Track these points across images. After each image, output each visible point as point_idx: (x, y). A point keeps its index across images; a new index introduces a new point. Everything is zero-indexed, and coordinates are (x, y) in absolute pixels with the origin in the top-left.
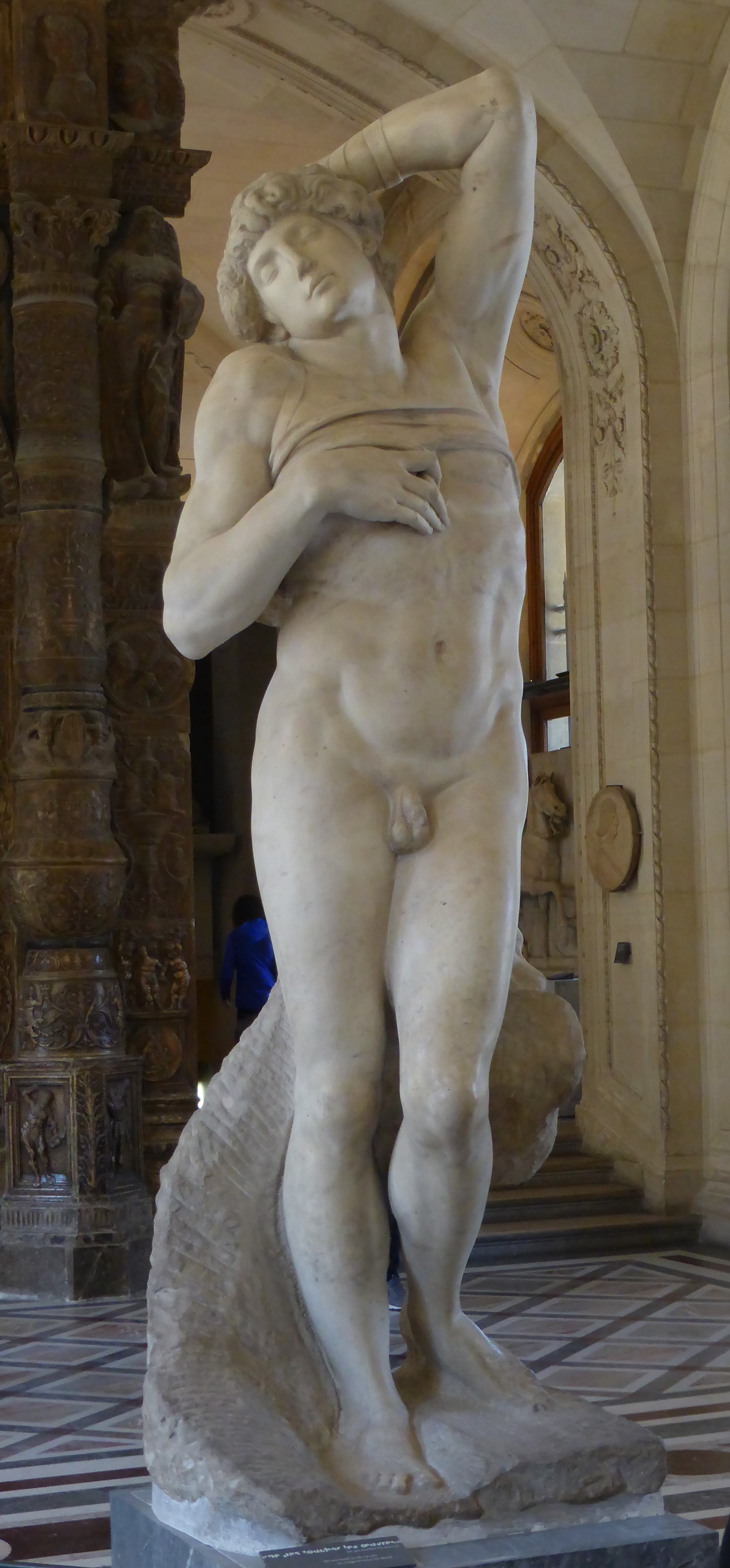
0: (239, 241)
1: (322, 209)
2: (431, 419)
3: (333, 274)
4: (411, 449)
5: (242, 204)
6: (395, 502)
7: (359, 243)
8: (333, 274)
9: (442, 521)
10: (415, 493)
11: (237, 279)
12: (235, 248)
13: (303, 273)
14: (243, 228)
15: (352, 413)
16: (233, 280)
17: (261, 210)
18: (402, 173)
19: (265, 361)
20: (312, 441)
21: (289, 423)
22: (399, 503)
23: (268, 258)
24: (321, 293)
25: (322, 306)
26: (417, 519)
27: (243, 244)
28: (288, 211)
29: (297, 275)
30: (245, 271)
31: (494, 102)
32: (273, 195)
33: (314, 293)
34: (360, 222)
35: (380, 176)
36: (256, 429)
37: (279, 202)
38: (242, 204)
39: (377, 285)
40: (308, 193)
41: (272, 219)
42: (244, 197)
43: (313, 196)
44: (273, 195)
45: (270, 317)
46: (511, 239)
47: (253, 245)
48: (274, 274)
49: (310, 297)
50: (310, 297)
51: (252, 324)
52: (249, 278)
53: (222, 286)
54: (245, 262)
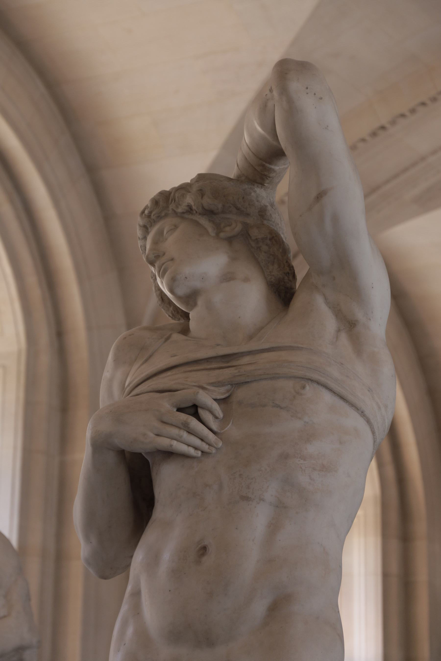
1: (180, 210)
2: (246, 360)
3: (172, 259)
4: (184, 389)
6: (151, 435)
7: (210, 230)
8: (172, 259)
9: (209, 445)
10: (172, 425)
12: (143, 253)
15: (165, 367)
18: (270, 163)
19: (125, 338)
22: (158, 435)
26: (171, 446)
28: (160, 218)
34: (209, 213)
35: (255, 169)
37: (150, 212)
39: (233, 259)
41: (148, 226)
43: (173, 202)
46: (320, 196)
51: (171, 309)
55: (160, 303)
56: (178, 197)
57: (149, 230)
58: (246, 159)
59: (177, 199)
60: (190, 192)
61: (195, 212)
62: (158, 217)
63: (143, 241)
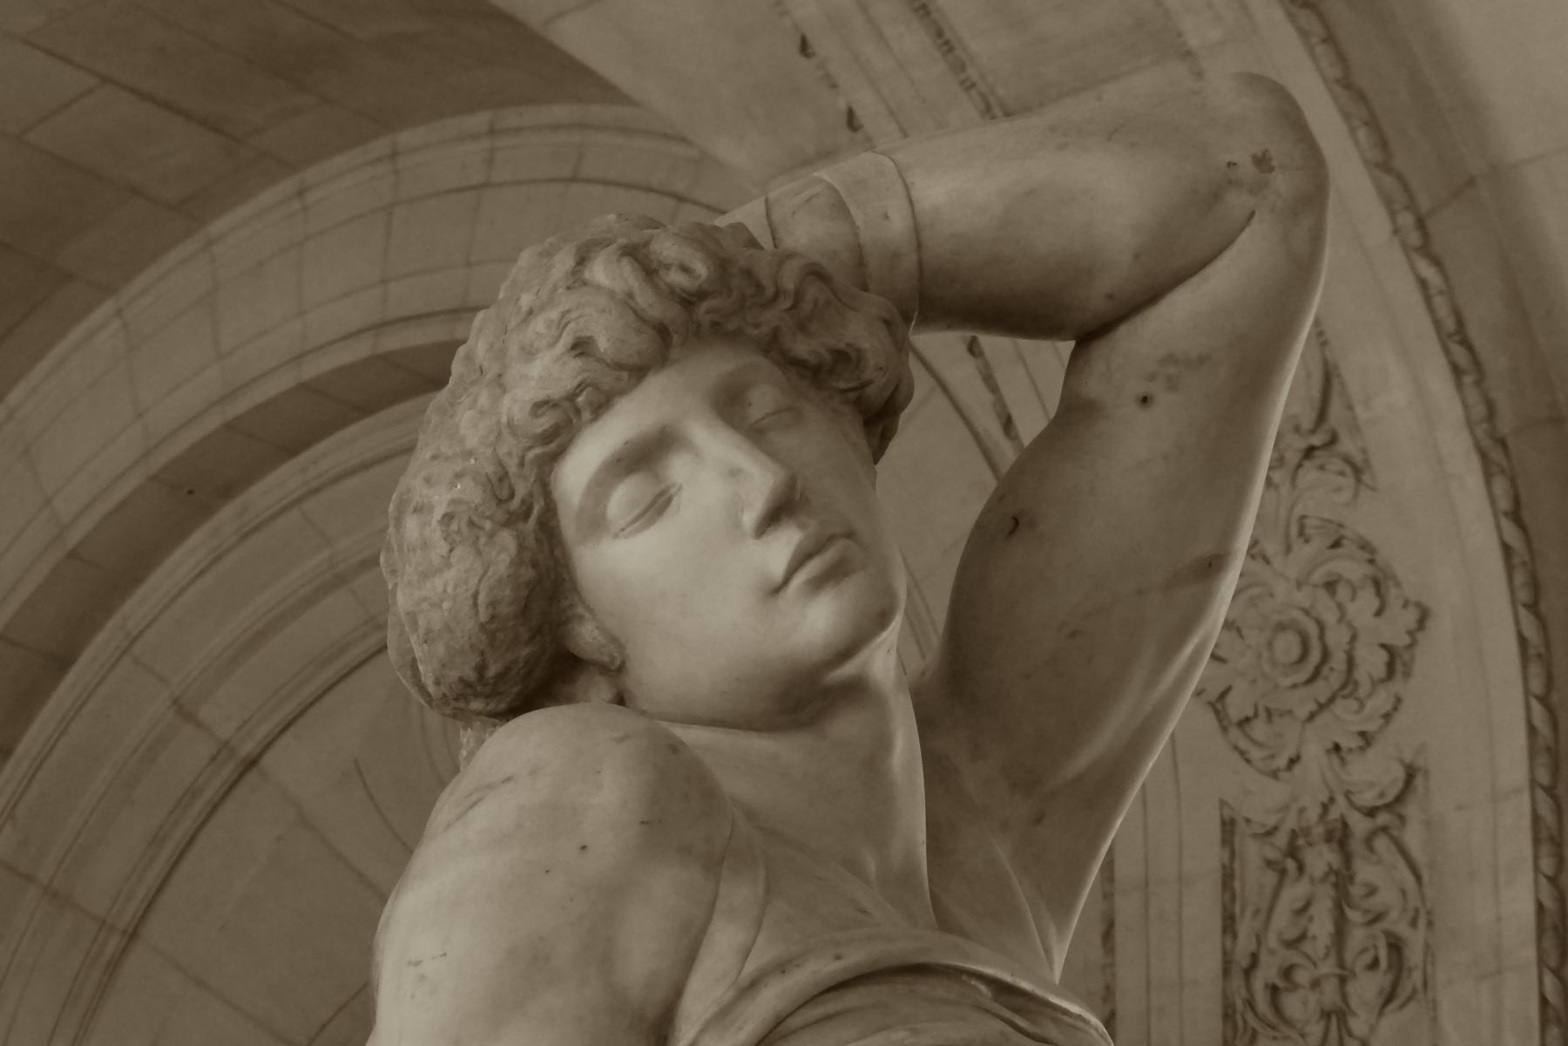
0: (568, 384)
1: (802, 348)
3: (850, 535)
5: (576, 279)
8: (850, 535)
11: (515, 504)
12: (539, 407)
13: (775, 516)
14: (581, 347)
16: (500, 502)
17: (645, 299)
20: (828, 1018)
21: (746, 953)
23: (646, 455)
24: (818, 584)
25: (816, 621)
27: (571, 397)
29: (750, 518)
30: (545, 486)
31: (1262, 162)
32: (685, 269)
33: (800, 578)
36: (641, 955)
37: (702, 294)
38: (576, 279)
40: (770, 291)
41: (676, 338)
42: (582, 261)
44: (685, 269)
45: (586, 637)
46: (1212, 566)
47: (600, 407)
48: (658, 506)
49: (777, 590)
50: (777, 590)
51: (525, 652)
52: (550, 509)
53: (448, 518)
54: (556, 457)
55: (505, 610)
56: (816, 303)
57: (675, 353)
58: (861, 262)
59: (807, 306)
60: (853, 309)
61: (842, 385)
62: (715, 324)
63: (625, 375)
